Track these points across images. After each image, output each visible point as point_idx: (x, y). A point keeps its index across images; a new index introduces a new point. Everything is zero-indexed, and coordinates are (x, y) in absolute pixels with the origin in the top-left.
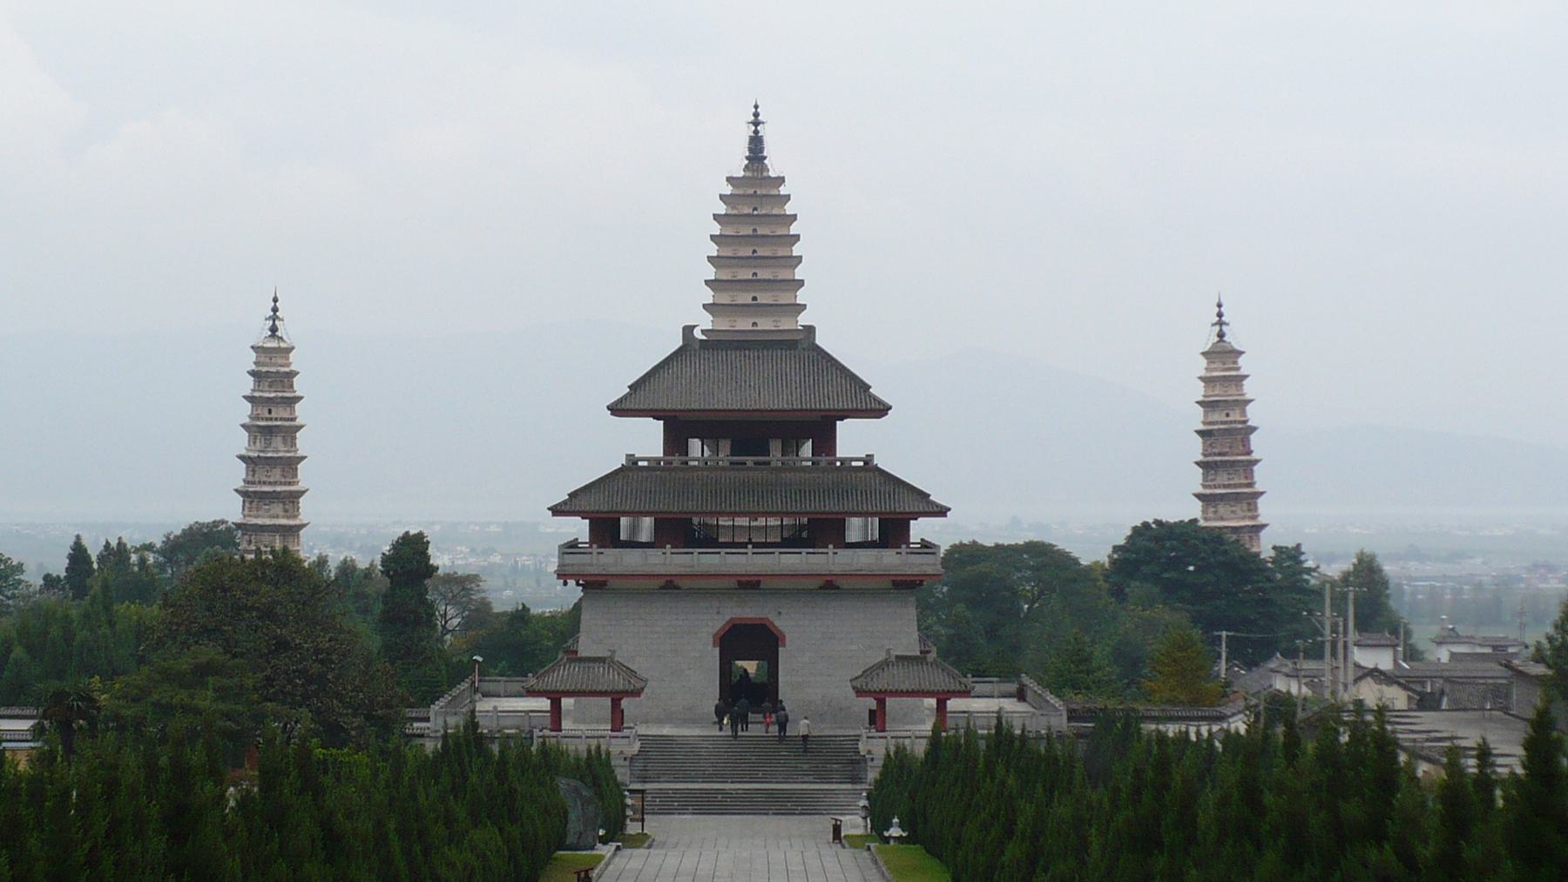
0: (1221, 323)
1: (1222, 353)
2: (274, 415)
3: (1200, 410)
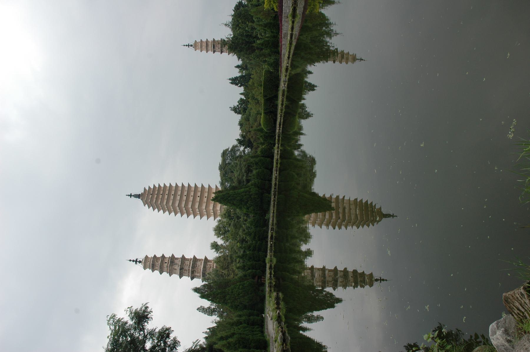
0: (189, 45)
1: (196, 46)
2: (167, 262)
3: (209, 52)
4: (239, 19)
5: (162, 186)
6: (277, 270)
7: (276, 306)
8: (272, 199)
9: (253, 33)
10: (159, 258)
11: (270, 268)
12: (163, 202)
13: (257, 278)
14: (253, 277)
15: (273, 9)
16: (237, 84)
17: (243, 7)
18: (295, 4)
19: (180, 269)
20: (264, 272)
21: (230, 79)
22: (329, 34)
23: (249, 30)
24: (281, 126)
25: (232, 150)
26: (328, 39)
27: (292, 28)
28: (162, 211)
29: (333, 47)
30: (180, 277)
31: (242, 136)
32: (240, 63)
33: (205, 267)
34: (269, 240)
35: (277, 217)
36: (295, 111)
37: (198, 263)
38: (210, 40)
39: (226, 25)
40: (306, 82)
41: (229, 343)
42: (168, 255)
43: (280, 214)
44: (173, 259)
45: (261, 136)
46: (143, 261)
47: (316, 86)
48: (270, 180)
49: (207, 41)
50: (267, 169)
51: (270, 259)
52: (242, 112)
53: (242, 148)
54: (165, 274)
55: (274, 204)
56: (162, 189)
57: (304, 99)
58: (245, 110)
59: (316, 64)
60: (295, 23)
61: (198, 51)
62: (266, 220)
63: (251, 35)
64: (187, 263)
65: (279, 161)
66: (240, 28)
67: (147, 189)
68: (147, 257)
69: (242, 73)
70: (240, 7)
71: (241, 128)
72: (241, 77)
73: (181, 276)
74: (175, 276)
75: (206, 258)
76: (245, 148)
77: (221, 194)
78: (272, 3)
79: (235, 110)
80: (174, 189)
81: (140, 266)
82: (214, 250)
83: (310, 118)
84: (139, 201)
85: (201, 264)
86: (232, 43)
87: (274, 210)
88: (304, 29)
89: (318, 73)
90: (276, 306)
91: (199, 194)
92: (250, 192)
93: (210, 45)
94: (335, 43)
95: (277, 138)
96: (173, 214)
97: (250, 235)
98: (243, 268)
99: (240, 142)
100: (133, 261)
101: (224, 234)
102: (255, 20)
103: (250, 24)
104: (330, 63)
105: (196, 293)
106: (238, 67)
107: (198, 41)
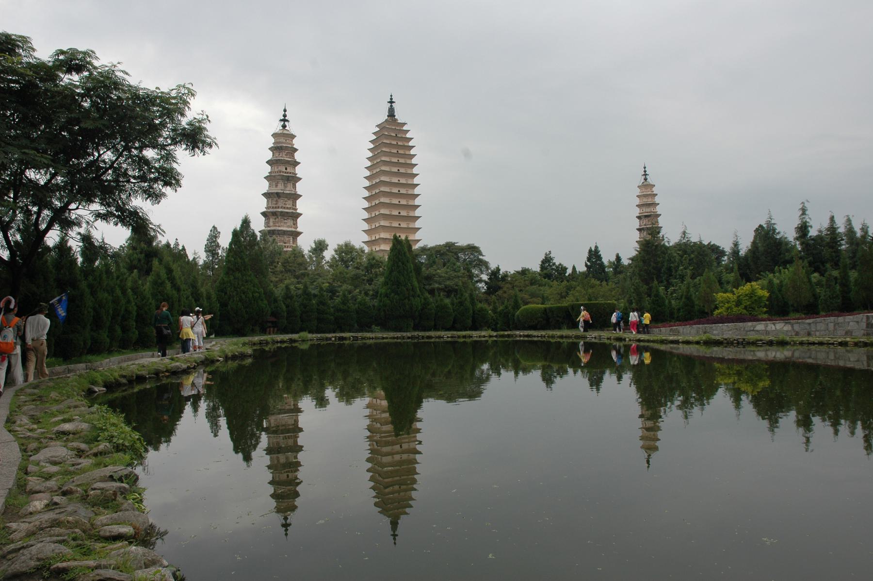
0: (645, 175)
2: (288, 170)
3: (638, 209)
4: (696, 253)
5: (412, 152)
6: (289, 352)
7: (230, 354)
8: (404, 334)
9: (675, 278)
10: (293, 156)
11: (292, 341)
12: (385, 156)
13: (273, 319)
14: (274, 314)
15: (716, 308)
16: (589, 259)
17: (717, 258)
18: (728, 343)
19: (277, 194)
20: (284, 331)
21: (596, 247)
22: (685, 405)
23: (680, 272)
24: (526, 339)
25: (481, 261)
26: (677, 403)
27: (688, 343)
28: (370, 154)
29: (665, 412)
30: (264, 195)
31: (506, 275)
32: (625, 261)
33: (284, 233)
34: (338, 335)
35: (376, 344)
36: (555, 359)
37: (290, 222)
38: (659, 210)
39: (684, 233)
40: (603, 373)
41: (163, 283)
42: (299, 171)
43: (381, 349)
44: (295, 179)
45: (506, 307)
46: (285, 132)
47: (598, 389)
48: (436, 328)
49: (656, 205)
50: (455, 322)
51: (306, 339)
52: (545, 272)
53: (485, 277)
54: (268, 168)
55: (397, 338)
56: (407, 153)
57: (575, 372)
58: (548, 276)
59: (633, 387)
60: (697, 346)
61: (638, 192)
62: (370, 327)
63: (671, 275)
64: (289, 204)
65: (468, 340)
66: (682, 257)
67: (405, 128)
68: (293, 137)
69: (609, 267)
70: (717, 253)
71: (518, 272)
72: (602, 265)
73: (266, 195)
74: (265, 186)
75: (299, 234)
76: (486, 283)
77: (406, 249)
78: (727, 305)
79: (547, 261)
80: (409, 171)
81: (277, 127)
82: (314, 246)
83: (544, 384)
84: (383, 117)
85: (288, 227)
86: (657, 246)
87: (387, 338)
88: (689, 361)
89: (620, 392)
90: (230, 354)
91: (404, 213)
92: (413, 296)
93: (648, 210)
94: (672, 415)
95: (506, 333)
96: (368, 173)
97: (344, 303)
98: (288, 296)
99: (495, 273)
100: (285, 116)
101: (342, 259)
102: (697, 280)
103: (689, 272)
104: (637, 409)
105: (240, 223)
106: (618, 258)
107: (654, 189)
